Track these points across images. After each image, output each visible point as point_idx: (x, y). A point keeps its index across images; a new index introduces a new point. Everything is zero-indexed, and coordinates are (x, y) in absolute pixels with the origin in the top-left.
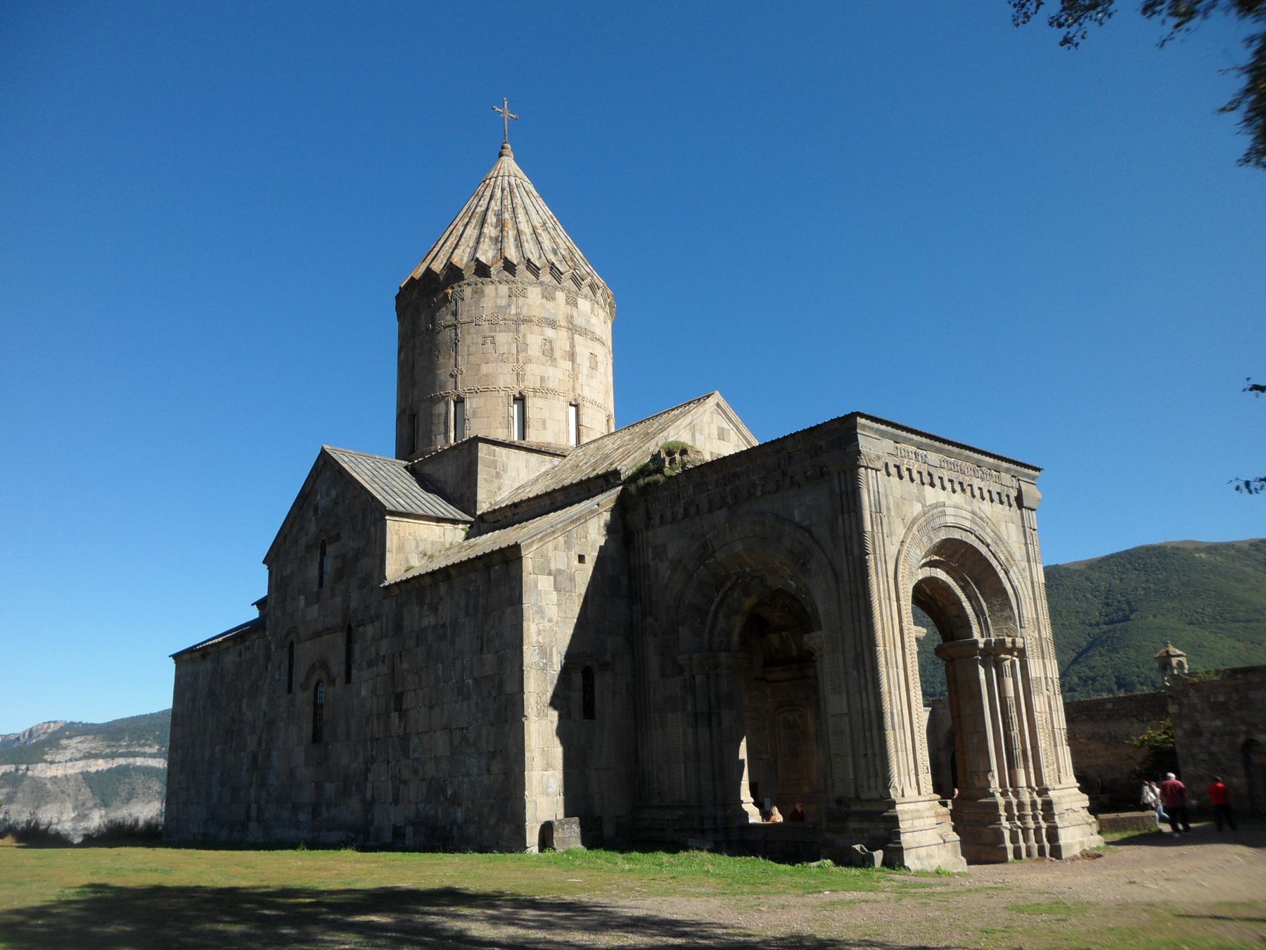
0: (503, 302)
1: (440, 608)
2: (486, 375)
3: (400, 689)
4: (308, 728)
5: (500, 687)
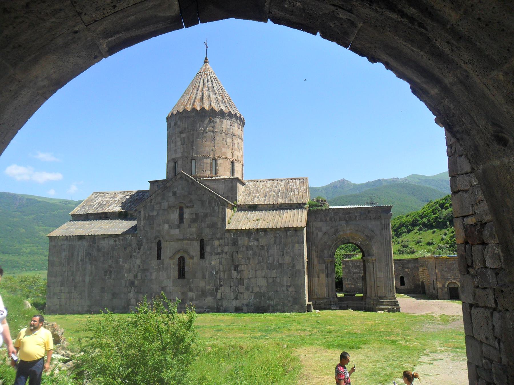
0: (229, 127)
1: (260, 240)
2: (224, 152)
3: (237, 264)
4: (175, 273)
5: (293, 266)
